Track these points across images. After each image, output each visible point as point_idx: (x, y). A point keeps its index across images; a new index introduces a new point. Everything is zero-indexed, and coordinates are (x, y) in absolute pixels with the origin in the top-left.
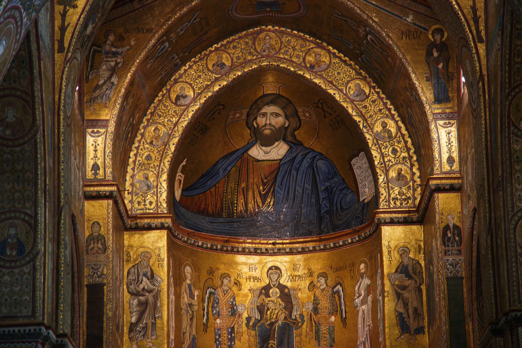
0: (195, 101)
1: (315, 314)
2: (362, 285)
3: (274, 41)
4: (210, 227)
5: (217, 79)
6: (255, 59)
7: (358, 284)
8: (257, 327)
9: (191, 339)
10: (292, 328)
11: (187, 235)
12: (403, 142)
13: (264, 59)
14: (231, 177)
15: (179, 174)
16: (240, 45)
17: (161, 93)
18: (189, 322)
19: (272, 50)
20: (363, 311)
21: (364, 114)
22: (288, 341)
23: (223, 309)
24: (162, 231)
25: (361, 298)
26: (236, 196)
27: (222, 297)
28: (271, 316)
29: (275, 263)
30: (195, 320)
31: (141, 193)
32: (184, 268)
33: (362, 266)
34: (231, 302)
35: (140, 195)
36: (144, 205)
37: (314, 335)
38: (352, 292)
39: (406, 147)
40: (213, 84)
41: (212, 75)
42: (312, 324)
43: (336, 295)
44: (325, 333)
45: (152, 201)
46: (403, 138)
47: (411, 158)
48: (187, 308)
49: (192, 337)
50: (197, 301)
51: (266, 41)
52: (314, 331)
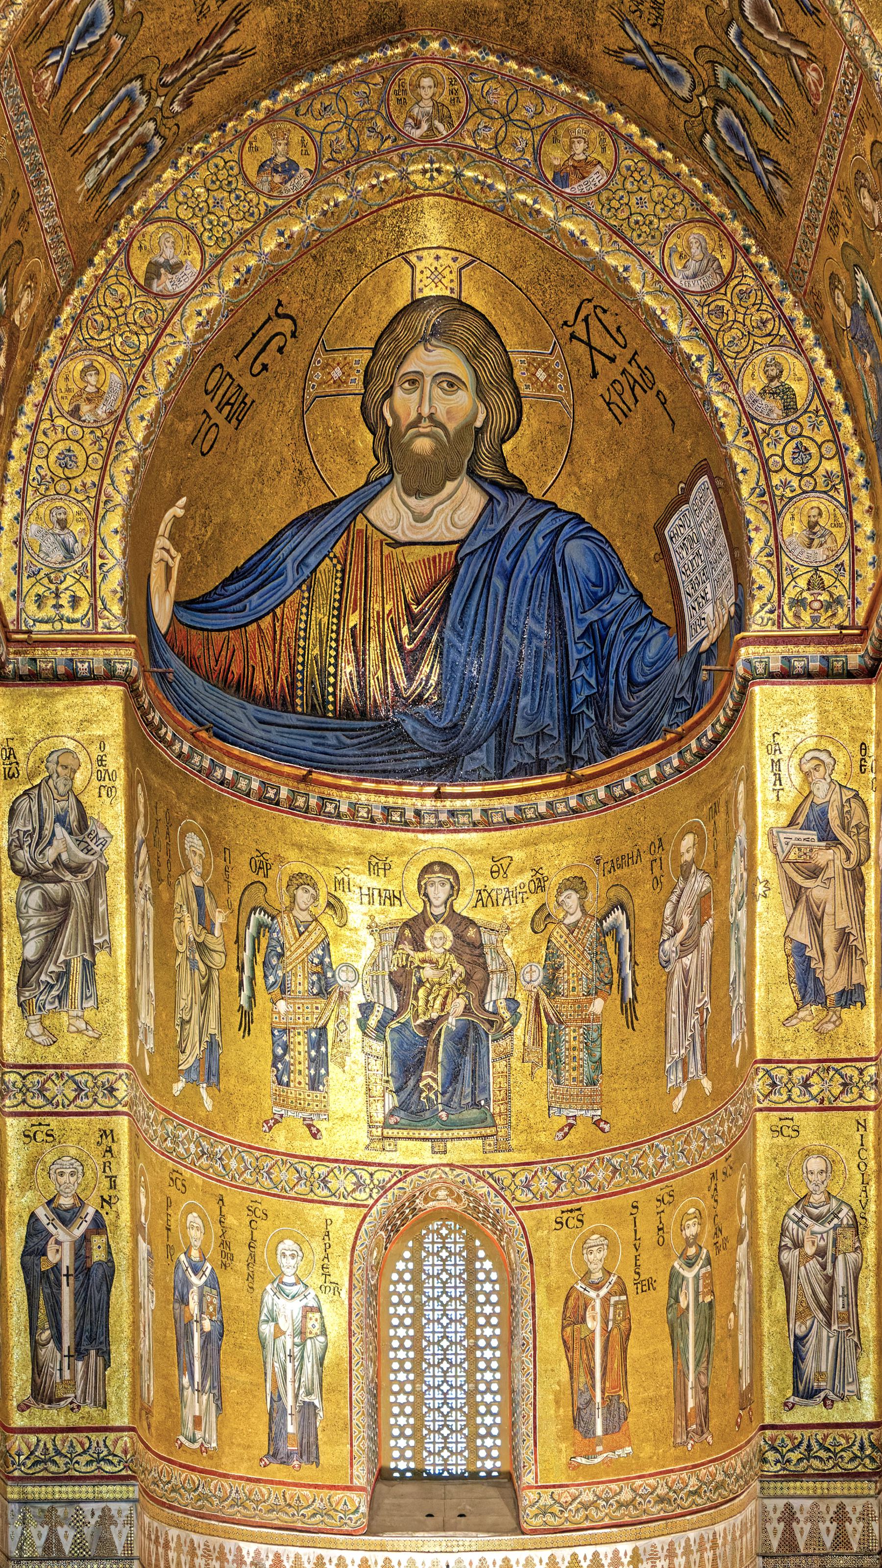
0: (206, 281)
1: (548, 995)
2: (683, 899)
3: (446, 92)
4: (257, 732)
5: (271, 213)
6: (389, 151)
7: (674, 898)
8: (388, 1030)
9: (204, 1045)
10: (484, 1037)
11: (189, 736)
12: (825, 428)
13: (417, 149)
14: (318, 590)
15: (162, 542)
16: (342, 105)
17: (102, 252)
18: (199, 997)
19: (441, 121)
20: (686, 973)
21: (713, 333)
22: (474, 1072)
23: (295, 975)
24: (109, 687)
25: (680, 936)
26: (333, 653)
27: (292, 941)
28: (427, 1002)
29: (441, 853)
30: (214, 991)
31: (45, 571)
32: (183, 835)
33: (689, 840)
34: (318, 956)
35: (42, 574)
36: (54, 606)
37: (545, 1057)
38: (655, 924)
39: (834, 442)
40: (258, 231)
41: (255, 201)
42: (539, 1027)
43: (608, 939)
44: (574, 1049)
45: (78, 594)
46: (828, 416)
47: (847, 475)
48: (192, 952)
49: (206, 1039)
50: (221, 940)
51: (423, 93)
52: (545, 1042)
